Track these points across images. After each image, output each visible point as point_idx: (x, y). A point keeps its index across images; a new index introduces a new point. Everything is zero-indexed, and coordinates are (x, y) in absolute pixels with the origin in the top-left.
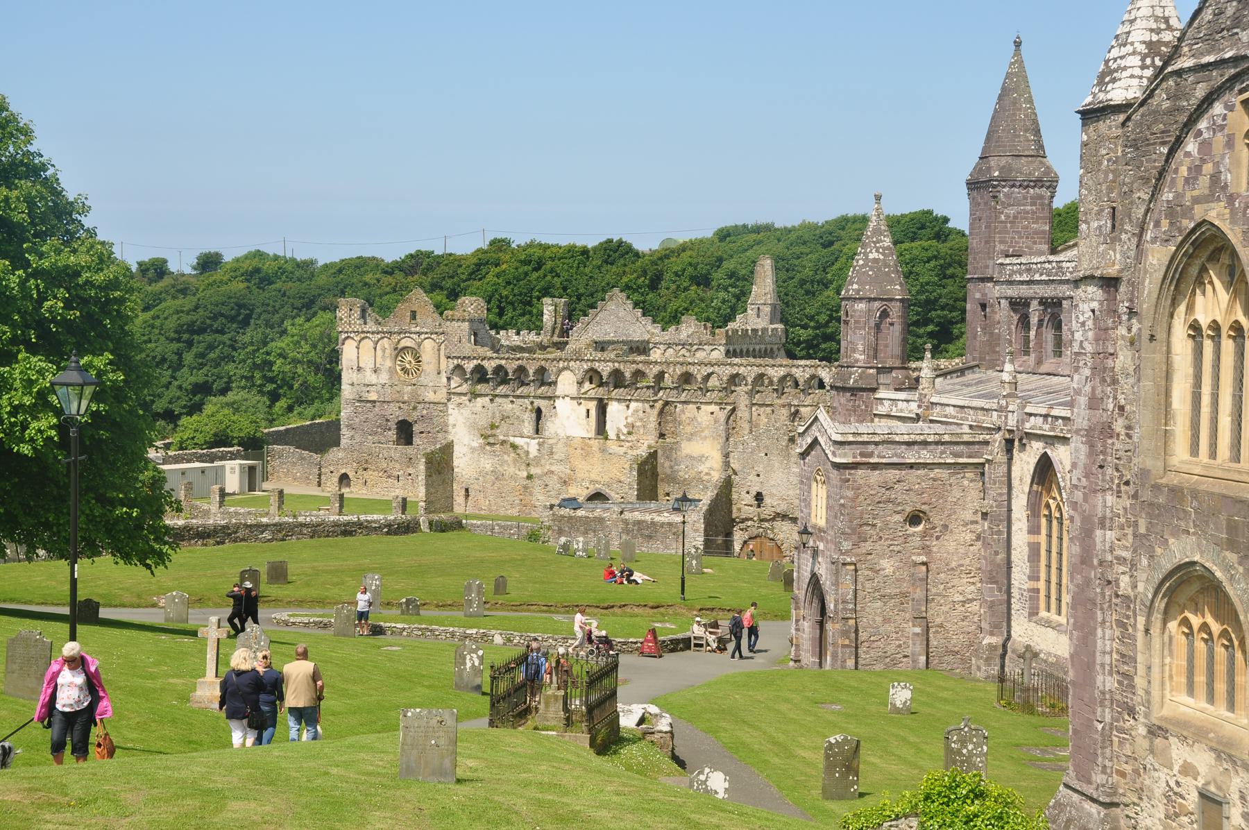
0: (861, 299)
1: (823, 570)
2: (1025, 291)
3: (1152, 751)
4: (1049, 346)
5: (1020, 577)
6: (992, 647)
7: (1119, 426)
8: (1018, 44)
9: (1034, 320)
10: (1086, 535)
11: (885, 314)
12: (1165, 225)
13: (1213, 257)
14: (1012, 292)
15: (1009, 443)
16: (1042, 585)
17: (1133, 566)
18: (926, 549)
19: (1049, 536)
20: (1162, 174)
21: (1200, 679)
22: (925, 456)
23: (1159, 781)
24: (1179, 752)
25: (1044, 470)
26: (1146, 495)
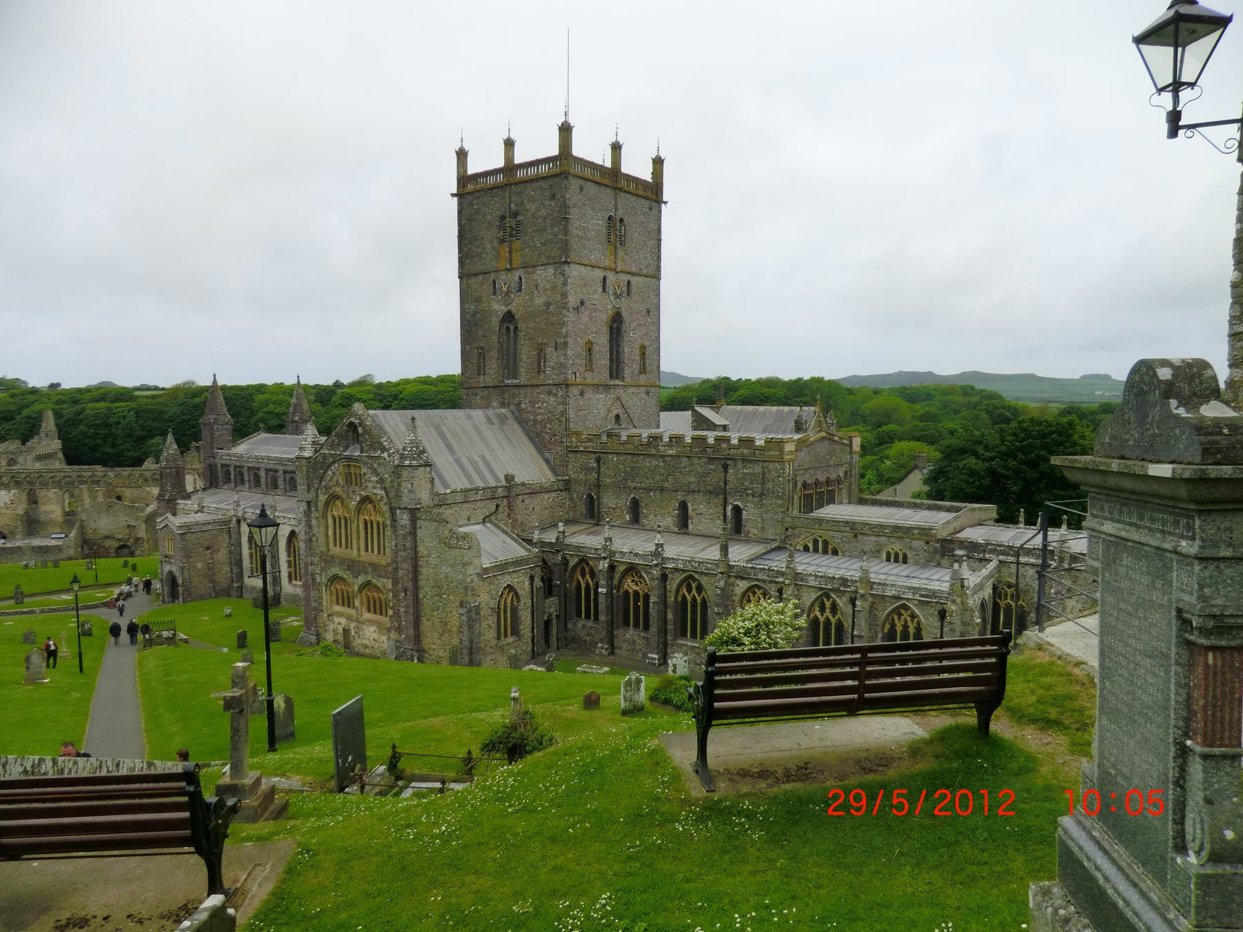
0: (167, 468)
1: (175, 569)
2: (228, 462)
3: (329, 620)
4: (239, 481)
6: (238, 587)
7: (314, 539)
8: (215, 375)
9: (233, 472)
10: (306, 566)
11: (177, 472)
12: (324, 490)
14: (223, 462)
15: (239, 521)
16: (254, 565)
18: (212, 558)
20: (322, 478)
21: (340, 601)
22: (210, 527)
23: (332, 627)
24: (336, 620)
26: (324, 557)
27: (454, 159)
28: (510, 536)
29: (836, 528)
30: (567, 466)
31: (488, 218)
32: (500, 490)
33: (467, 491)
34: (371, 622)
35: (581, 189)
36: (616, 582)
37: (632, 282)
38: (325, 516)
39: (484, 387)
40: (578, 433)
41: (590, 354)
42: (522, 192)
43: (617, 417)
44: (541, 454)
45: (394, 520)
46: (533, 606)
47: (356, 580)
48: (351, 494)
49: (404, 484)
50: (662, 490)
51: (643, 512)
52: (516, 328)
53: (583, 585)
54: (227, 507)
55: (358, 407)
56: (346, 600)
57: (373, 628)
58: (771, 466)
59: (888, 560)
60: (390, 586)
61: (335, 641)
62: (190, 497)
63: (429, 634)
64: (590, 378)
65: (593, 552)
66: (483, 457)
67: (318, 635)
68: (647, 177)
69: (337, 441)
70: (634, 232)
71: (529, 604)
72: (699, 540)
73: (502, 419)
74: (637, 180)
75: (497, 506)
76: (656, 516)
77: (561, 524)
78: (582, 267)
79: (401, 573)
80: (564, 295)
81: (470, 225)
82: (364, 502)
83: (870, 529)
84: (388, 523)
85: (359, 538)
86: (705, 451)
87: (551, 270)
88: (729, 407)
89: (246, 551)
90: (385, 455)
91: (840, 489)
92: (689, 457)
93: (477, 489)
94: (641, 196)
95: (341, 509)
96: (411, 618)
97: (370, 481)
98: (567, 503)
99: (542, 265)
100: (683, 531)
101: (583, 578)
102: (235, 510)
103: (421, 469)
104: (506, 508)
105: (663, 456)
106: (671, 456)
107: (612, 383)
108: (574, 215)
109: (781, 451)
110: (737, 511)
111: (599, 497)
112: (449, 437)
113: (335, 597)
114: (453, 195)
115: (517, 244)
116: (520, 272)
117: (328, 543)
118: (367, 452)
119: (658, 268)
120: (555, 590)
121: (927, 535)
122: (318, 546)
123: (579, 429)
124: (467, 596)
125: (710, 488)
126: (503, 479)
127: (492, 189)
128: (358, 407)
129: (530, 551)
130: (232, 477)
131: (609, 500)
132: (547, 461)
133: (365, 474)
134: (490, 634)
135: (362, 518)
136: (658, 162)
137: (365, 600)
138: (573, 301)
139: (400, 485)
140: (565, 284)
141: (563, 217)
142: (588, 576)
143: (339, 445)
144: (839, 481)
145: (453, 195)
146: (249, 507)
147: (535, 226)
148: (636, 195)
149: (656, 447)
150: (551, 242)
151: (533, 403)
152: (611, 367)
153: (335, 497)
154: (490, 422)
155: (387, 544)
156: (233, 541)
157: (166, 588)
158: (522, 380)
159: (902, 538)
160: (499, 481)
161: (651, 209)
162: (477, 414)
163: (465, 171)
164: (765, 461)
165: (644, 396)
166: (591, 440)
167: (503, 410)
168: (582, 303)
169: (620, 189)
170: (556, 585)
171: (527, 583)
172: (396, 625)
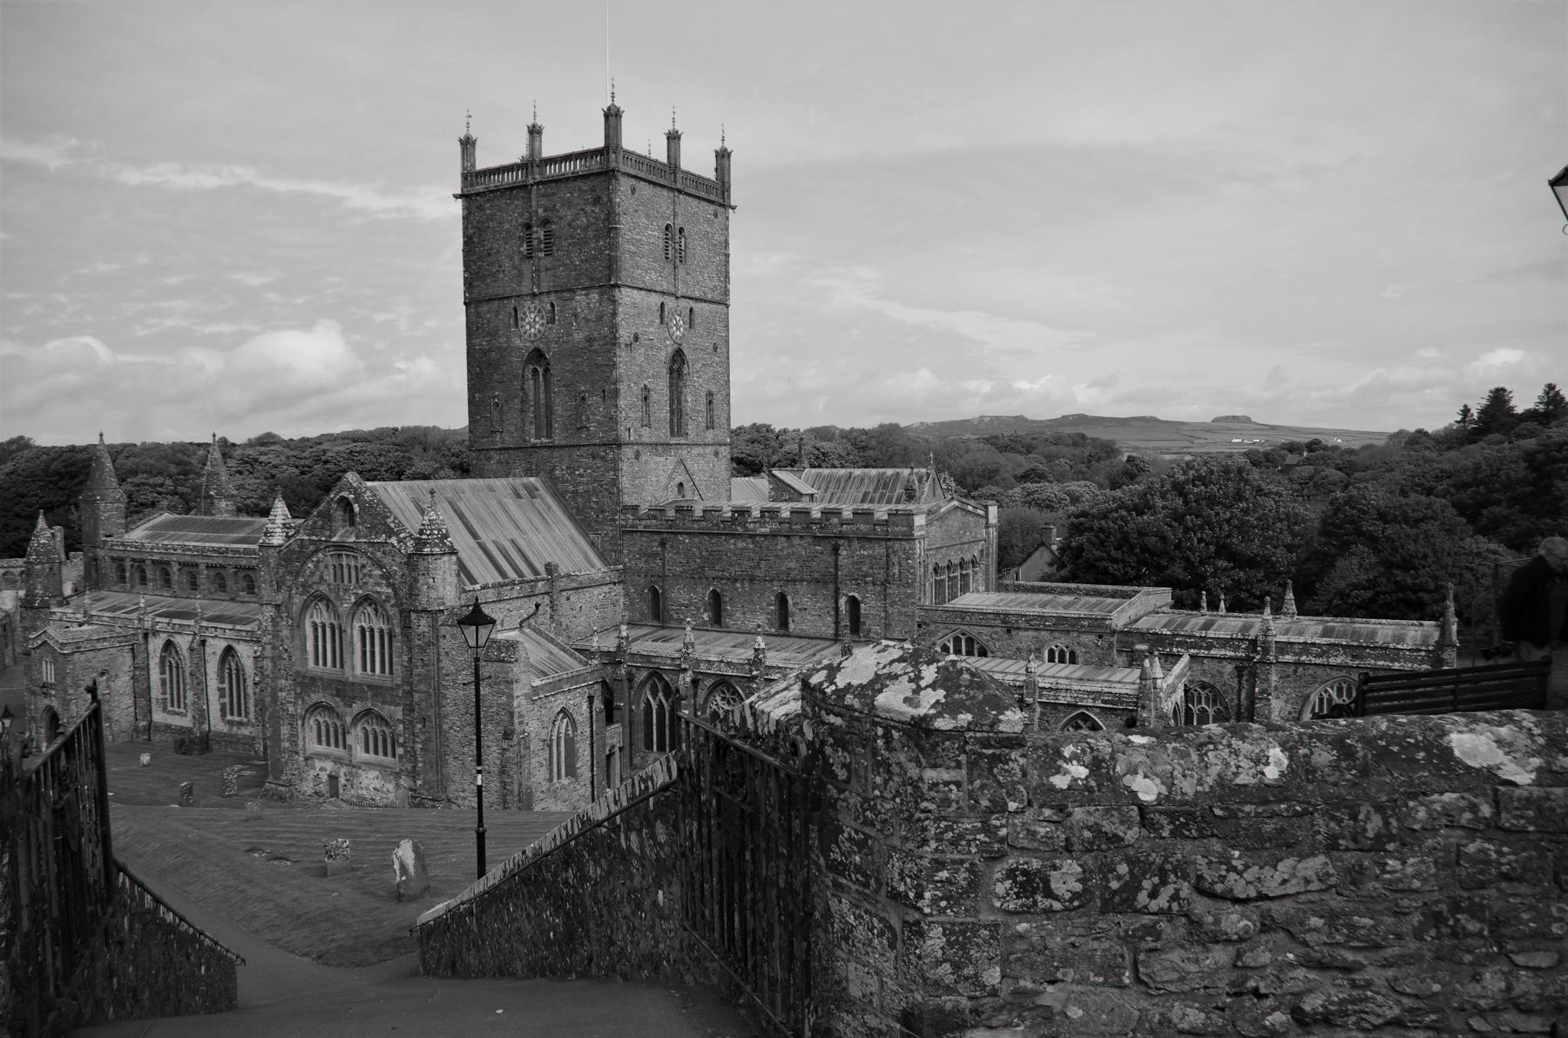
1: (55, 704)
2: (121, 554)
5: (156, 692)
7: (285, 656)
8: (101, 435)
9: (128, 568)
11: (51, 569)
12: (301, 589)
13: (321, 600)
15: (146, 636)
16: (168, 696)
17: (295, 704)
18: (109, 687)
19: (171, 674)
20: (297, 574)
21: (324, 739)
22: (106, 644)
24: (318, 764)
25: (169, 645)
26: (300, 680)
27: (458, 148)
28: (557, 645)
29: (983, 622)
30: (621, 552)
31: (507, 226)
32: (540, 584)
33: (501, 585)
34: (370, 765)
35: (633, 190)
36: (700, 700)
37: (695, 310)
38: (299, 625)
39: (502, 449)
40: (635, 508)
41: (647, 405)
42: (554, 194)
43: (681, 485)
44: (585, 535)
45: (407, 626)
46: (592, 736)
47: (348, 710)
48: (341, 593)
49: (421, 580)
50: (752, 579)
51: (726, 610)
52: (547, 371)
53: (655, 707)
54: (128, 616)
55: (351, 477)
56: (338, 736)
57: (373, 774)
58: (897, 545)
59: (1051, 659)
60: (399, 716)
61: (316, 793)
62: (68, 604)
63: (457, 778)
64: (647, 435)
65: (669, 662)
66: (513, 542)
67: (289, 784)
68: (711, 175)
69: (320, 523)
70: (697, 248)
71: (588, 733)
72: (804, 642)
73: (532, 492)
74: (697, 180)
75: (537, 606)
76: (744, 613)
77: (624, 627)
78: (636, 292)
79: (416, 696)
80: (614, 328)
81: (480, 235)
82: (361, 604)
83: (1027, 621)
84: (398, 630)
85: (353, 653)
86: (808, 527)
87: (595, 296)
88: (813, 470)
89: (155, 676)
90: (394, 540)
91: (975, 573)
92: (788, 537)
93: (513, 583)
94: (704, 199)
95: (325, 614)
96: (433, 757)
97: (370, 576)
98: (622, 600)
99: (583, 289)
100: (782, 632)
101: (654, 698)
102: (140, 620)
103: (446, 558)
104: (548, 608)
105: (752, 536)
106: (764, 535)
107: (674, 441)
108: (624, 224)
109: (911, 526)
110: (854, 604)
111: (664, 591)
112: (467, 514)
113: (315, 734)
114: (456, 197)
115: (547, 262)
116: (553, 298)
117: (306, 659)
118: (365, 537)
119: (726, 292)
120: (616, 714)
121: (1099, 626)
122: (293, 664)
123: (635, 503)
124: (512, 723)
125: (816, 575)
126: (541, 569)
127: (511, 189)
128: (351, 477)
129: (586, 664)
130: (128, 574)
131: (679, 595)
132: (592, 544)
133: (363, 566)
134: (540, 776)
135: (357, 625)
136: (723, 156)
137: (361, 735)
138: (624, 334)
139: (416, 581)
140: (614, 314)
141: (608, 227)
142: (661, 695)
143: (322, 527)
144: (974, 563)
145: (456, 197)
146: (159, 615)
147: (573, 237)
148: (698, 198)
149: (743, 524)
150: (595, 258)
151: (570, 469)
152: (671, 420)
153: (321, 597)
154: (519, 496)
155: (395, 660)
156: (139, 660)
157: (42, 730)
158: (558, 439)
159: (1068, 631)
160: (536, 572)
161: (716, 215)
162: (498, 483)
163: (473, 165)
164: (889, 540)
165: (712, 457)
166: (655, 517)
167: (532, 479)
168: (636, 338)
169: (680, 191)
170: (619, 708)
171: (585, 706)
172: (409, 768)
